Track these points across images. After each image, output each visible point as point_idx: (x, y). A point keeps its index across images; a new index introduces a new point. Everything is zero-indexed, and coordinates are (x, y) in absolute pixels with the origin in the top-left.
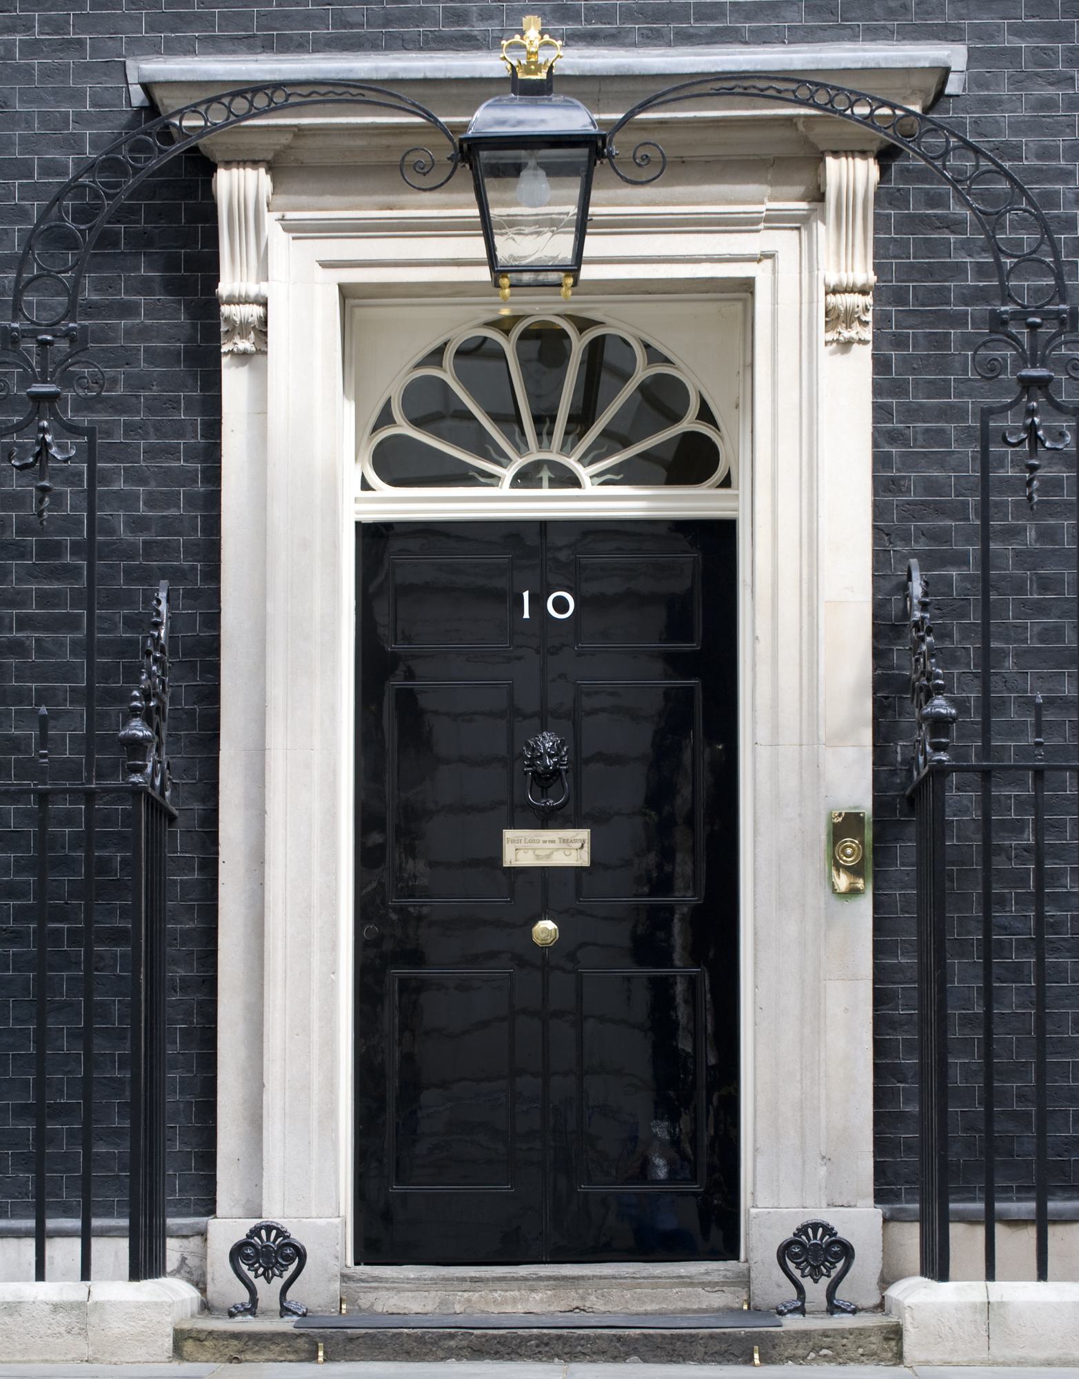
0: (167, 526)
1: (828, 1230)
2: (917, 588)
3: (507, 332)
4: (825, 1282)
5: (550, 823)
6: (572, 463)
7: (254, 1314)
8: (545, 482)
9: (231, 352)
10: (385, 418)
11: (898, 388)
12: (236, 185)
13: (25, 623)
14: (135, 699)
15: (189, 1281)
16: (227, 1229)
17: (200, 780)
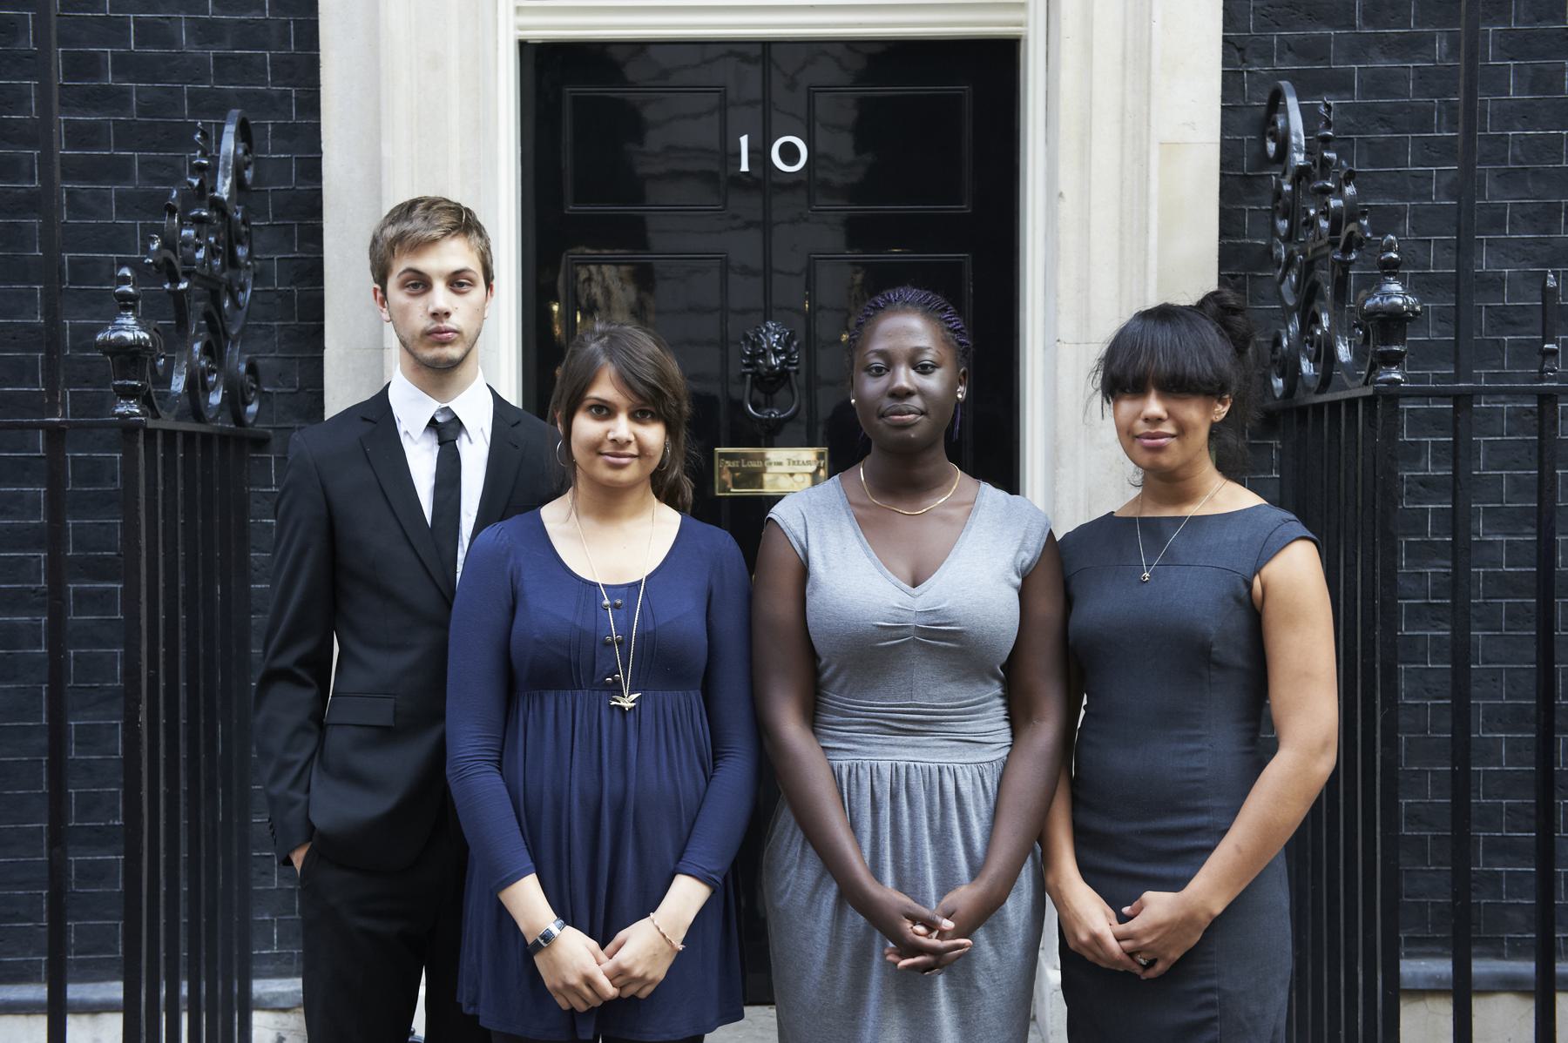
5: (777, 439)
14: (125, 280)
17: (301, 389)
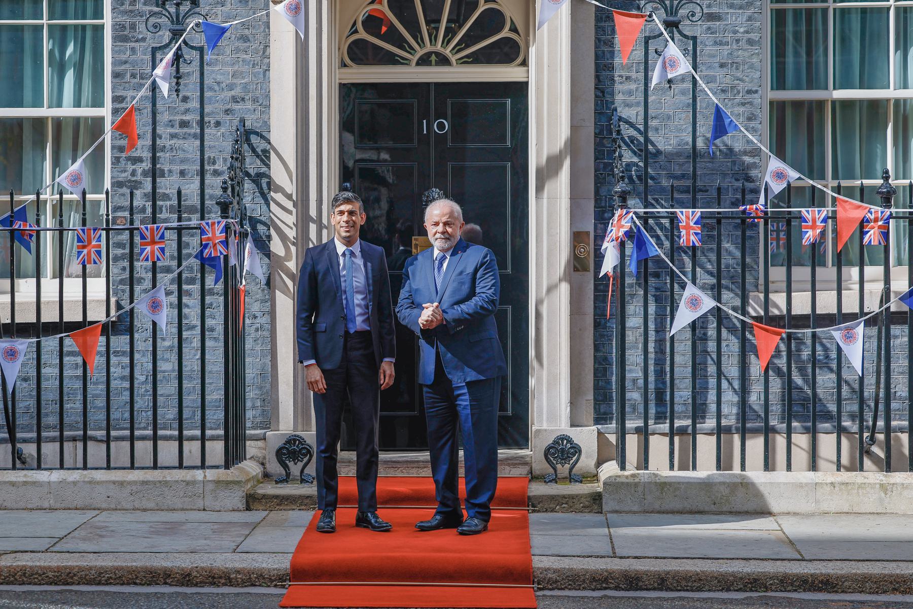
0: (245, 87)
1: (570, 440)
4: (567, 466)
6: (447, 52)
7: (287, 482)
8: (433, 62)
13: (173, 136)
15: (258, 461)
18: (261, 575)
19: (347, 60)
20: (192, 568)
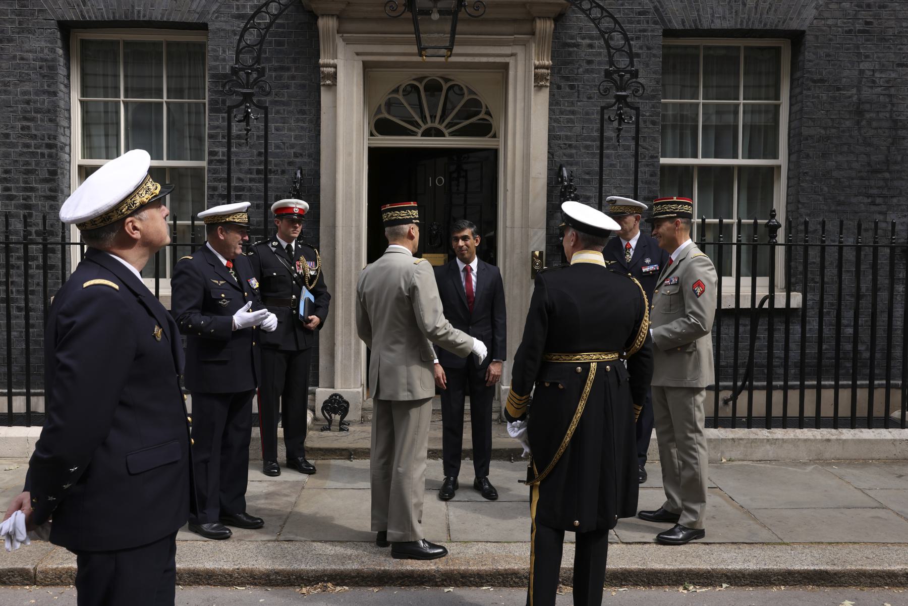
2: (565, 174)
3: (421, 83)
6: (442, 127)
7: (330, 430)
9: (324, 85)
10: (379, 111)
11: (558, 104)
12: (326, 24)
13: (251, 180)
16: (322, 394)
18: (300, 576)
19: (375, 132)
20: (234, 570)
